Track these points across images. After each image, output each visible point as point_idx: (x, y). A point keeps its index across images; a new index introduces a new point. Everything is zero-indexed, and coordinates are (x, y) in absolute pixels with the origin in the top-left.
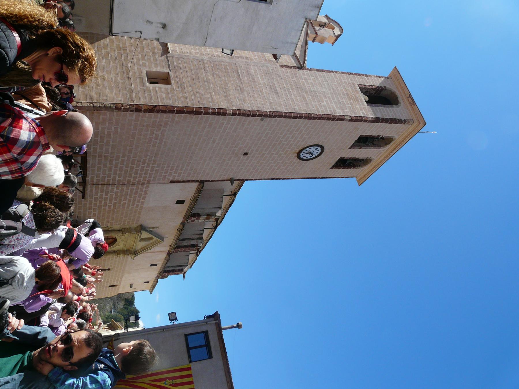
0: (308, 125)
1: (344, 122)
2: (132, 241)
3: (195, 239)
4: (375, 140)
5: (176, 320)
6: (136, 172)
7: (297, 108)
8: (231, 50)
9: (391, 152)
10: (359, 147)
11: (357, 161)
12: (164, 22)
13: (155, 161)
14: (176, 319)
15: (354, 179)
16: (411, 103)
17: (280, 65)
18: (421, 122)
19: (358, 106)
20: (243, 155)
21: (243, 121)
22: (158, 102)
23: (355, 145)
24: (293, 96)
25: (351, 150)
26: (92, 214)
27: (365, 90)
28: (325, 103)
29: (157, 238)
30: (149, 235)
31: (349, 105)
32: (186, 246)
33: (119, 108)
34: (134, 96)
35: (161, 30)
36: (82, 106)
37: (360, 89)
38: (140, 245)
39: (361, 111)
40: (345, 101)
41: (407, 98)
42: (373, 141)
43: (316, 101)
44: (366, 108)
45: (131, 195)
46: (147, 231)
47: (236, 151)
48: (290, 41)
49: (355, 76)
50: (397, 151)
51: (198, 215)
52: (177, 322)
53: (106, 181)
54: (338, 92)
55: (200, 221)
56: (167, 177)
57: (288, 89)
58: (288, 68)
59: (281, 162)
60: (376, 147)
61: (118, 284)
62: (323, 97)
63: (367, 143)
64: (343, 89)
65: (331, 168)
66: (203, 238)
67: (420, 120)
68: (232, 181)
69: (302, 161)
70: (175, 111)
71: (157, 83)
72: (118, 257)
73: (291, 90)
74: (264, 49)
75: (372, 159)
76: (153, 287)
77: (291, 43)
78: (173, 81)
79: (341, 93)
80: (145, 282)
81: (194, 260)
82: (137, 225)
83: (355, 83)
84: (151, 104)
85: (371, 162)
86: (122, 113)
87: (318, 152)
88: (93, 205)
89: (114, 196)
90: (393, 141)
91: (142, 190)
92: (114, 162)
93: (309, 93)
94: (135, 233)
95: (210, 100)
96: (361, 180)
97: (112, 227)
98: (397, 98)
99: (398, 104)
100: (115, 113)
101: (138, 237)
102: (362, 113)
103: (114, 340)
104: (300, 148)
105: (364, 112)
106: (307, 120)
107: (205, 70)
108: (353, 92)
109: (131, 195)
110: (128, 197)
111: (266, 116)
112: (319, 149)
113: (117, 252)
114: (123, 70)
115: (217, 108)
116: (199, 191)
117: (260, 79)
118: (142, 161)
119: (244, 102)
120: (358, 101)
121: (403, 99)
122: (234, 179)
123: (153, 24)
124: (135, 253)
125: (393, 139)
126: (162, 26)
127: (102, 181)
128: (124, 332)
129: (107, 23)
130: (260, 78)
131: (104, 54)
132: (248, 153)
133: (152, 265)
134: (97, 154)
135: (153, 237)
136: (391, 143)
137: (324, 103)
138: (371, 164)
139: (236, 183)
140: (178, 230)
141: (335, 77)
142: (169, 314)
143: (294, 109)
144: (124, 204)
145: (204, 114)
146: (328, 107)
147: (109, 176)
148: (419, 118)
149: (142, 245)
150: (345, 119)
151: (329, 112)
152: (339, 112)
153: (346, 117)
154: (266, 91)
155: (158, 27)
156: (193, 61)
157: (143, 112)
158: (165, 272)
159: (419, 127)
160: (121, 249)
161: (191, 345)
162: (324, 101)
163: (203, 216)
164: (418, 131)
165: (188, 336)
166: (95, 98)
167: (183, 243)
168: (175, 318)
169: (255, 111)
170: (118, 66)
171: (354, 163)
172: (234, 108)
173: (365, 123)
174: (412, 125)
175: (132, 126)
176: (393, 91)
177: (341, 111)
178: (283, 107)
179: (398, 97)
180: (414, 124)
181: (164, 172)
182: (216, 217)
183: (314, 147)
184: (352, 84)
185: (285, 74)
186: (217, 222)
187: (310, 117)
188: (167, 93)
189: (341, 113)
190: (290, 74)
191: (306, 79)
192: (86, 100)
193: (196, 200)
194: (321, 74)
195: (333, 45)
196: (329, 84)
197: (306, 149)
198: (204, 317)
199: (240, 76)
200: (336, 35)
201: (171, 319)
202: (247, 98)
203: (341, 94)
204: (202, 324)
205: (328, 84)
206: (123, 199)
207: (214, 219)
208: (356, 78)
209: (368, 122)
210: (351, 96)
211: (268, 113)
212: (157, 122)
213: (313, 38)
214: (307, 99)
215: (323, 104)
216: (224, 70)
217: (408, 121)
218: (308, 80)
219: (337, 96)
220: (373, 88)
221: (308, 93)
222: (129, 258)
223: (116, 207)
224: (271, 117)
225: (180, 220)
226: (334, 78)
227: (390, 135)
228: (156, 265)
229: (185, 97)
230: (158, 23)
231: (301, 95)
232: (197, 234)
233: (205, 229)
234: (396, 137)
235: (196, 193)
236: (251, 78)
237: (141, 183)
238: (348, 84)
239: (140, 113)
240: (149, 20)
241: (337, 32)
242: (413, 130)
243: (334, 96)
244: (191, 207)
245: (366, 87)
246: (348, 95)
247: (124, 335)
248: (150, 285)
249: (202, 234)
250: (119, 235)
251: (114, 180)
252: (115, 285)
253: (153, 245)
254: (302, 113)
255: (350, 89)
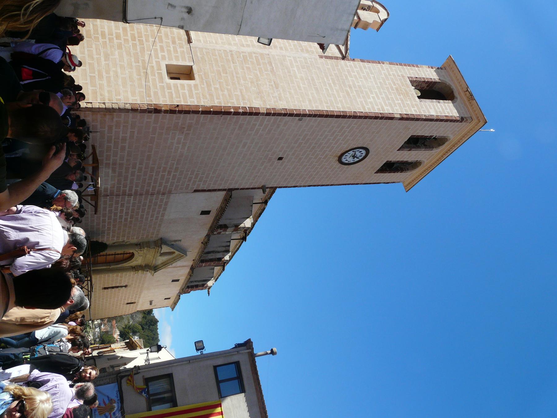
0: (353, 125)
1: (394, 121)
2: (152, 255)
3: (221, 252)
4: (427, 141)
5: (204, 350)
6: (155, 182)
7: (340, 105)
8: (269, 39)
9: (444, 154)
10: (409, 149)
11: (405, 164)
12: (189, 5)
13: (177, 169)
14: (203, 348)
15: (401, 184)
16: (469, 97)
17: (319, 55)
18: (481, 120)
19: (409, 102)
20: (277, 159)
21: (279, 122)
22: (180, 101)
23: (404, 146)
24: (335, 91)
25: (399, 152)
26: (106, 228)
27: (417, 83)
28: (372, 100)
29: (178, 252)
30: (169, 249)
31: (399, 101)
32: (211, 260)
33: (136, 108)
34: (152, 94)
35: (186, 16)
36: (92, 108)
37: (411, 83)
38: (161, 260)
39: (412, 107)
40: (394, 98)
41: (465, 92)
42: (424, 143)
43: (361, 97)
44: (418, 104)
45: (149, 207)
46: (168, 244)
47: (269, 156)
48: (340, 27)
49: (405, 67)
50: (452, 153)
51: (225, 227)
52: (205, 352)
53: (121, 192)
54: (386, 86)
55: (227, 233)
56: (190, 186)
57: (330, 85)
58: (328, 59)
59: (320, 167)
60: (428, 148)
61: (136, 301)
62: (369, 93)
63: (418, 144)
64: (391, 83)
65: (375, 173)
66: (229, 250)
67: (480, 118)
68: (264, 188)
69: (343, 166)
70: (200, 112)
71: (179, 79)
72: (136, 273)
73: (332, 85)
74: (309, 38)
75: (422, 162)
76: (175, 303)
77: (342, 30)
78: (196, 76)
79: (389, 87)
80: (165, 299)
81: (219, 274)
82: (156, 239)
83: (404, 75)
84: (171, 103)
85: (420, 165)
86: (139, 115)
87: (361, 155)
88: (107, 219)
89: (131, 208)
90: (447, 141)
91: (162, 200)
92: (131, 170)
93: (353, 88)
94: (154, 248)
95: (240, 98)
96: (409, 185)
97: (129, 242)
98: (453, 92)
99: (454, 99)
100: (131, 115)
101: (158, 252)
102: (414, 110)
103: (135, 374)
104: (342, 151)
105: (416, 109)
106: (351, 119)
107: (233, 63)
108: (403, 86)
109: (149, 207)
110: (146, 209)
111: (305, 115)
112: (364, 152)
113: (136, 268)
114: (137, 64)
115: (248, 106)
116: (227, 200)
117: (297, 73)
118: (162, 168)
119: (280, 100)
120: (409, 96)
121: (459, 93)
122: (266, 186)
123: (176, 8)
124: (155, 269)
125: (447, 139)
126: (186, 10)
127: (117, 192)
128: (145, 364)
129: (120, 8)
130: (296, 71)
131: (117, 45)
132: (283, 157)
133: (173, 281)
134: (111, 162)
135: (174, 251)
136: (445, 144)
137: (371, 99)
138: (420, 167)
139: (268, 190)
140: (202, 243)
141: (382, 68)
142: (195, 342)
143: (337, 107)
144: (142, 217)
145: (233, 115)
146: (376, 105)
147: (125, 186)
148: (478, 115)
149: (163, 260)
150: (394, 118)
151: (376, 109)
152: (387, 110)
153: (396, 116)
154: (304, 86)
155: (182, 12)
156: (219, 52)
157: (162, 113)
158: (188, 287)
159: (479, 125)
160: (140, 264)
161: (220, 379)
162: (371, 97)
163: (231, 227)
164: (477, 130)
165: (217, 368)
166: (107, 98)
167: (207, 256)
168: (203, 347)
169: (293, 110)
170: (133, 60)
171: (401, 167)
172: (269, 107)
173: (418, 121)
174: (470, 123)
175: (151, 130)
176: (448, 84)
177: (390, 109)
178: (324, 104)
179: (454, 92)
180: (473, 121)
181: (187, 180)
182: (245, 229)
183: (358, 150)
184: (401, 76)
185: (325, 66)
186: (246, 233)
187: (355, 117)
188: (190, 91)
189: (390, 110)
190: (331, 66)
191: (349, 72)
192: (97, 101)
193: (223, 210)
194: (367, 66)
195: (377, 32)
196: (376, 77)
197: (349, 153)
198: (235, 345)
199: (274, 68)
200: (381, 20)
201: (198, 348)
202: (282, 95)
203: (389, 88)
204: (233, 353)
205: (374, 77)
206: (140, 211)
207: (243, 231)
208: (406, 70)
209: (421, 121)
210: (401, 90)
211: (307, 112)
212: (180, 124)
213: (356, 24)
214: (351, 95)
215: (369, 100)
216: (255, 62)
217: (466, 119)
218: (351, 73)
219: (385, 91)
220: (425, 81)
221: (352, 88)
222: (149, 274)
223: (134, 219)
224: (311, 117)
225: (205, 233)
226: (381, 69)
227: (445, 135)
228: (178, 280)
229: (211, 95)
230: (182, 7)
231: (344, 90)
232: (223, 247)
233: (231, 241)
234: (451, 137)
235: (223, 203)
236: (286, 71)
237: (161, 193)
238: (397, 76)
239: (160, 114)
240: (171, 3)
241: (383, 15)
242: (471, 129)
243: (382, 90)
244: (217, 218)
245: (417, 79)
246: (397, 89)
247: (145, 368)
248: (171, 301)
249: (229, 246)
250: (137, 250)
251: (130, 190)
252: (133, 302)
253: (174, 260)
254: (346, 111)
255: (399, 82)
